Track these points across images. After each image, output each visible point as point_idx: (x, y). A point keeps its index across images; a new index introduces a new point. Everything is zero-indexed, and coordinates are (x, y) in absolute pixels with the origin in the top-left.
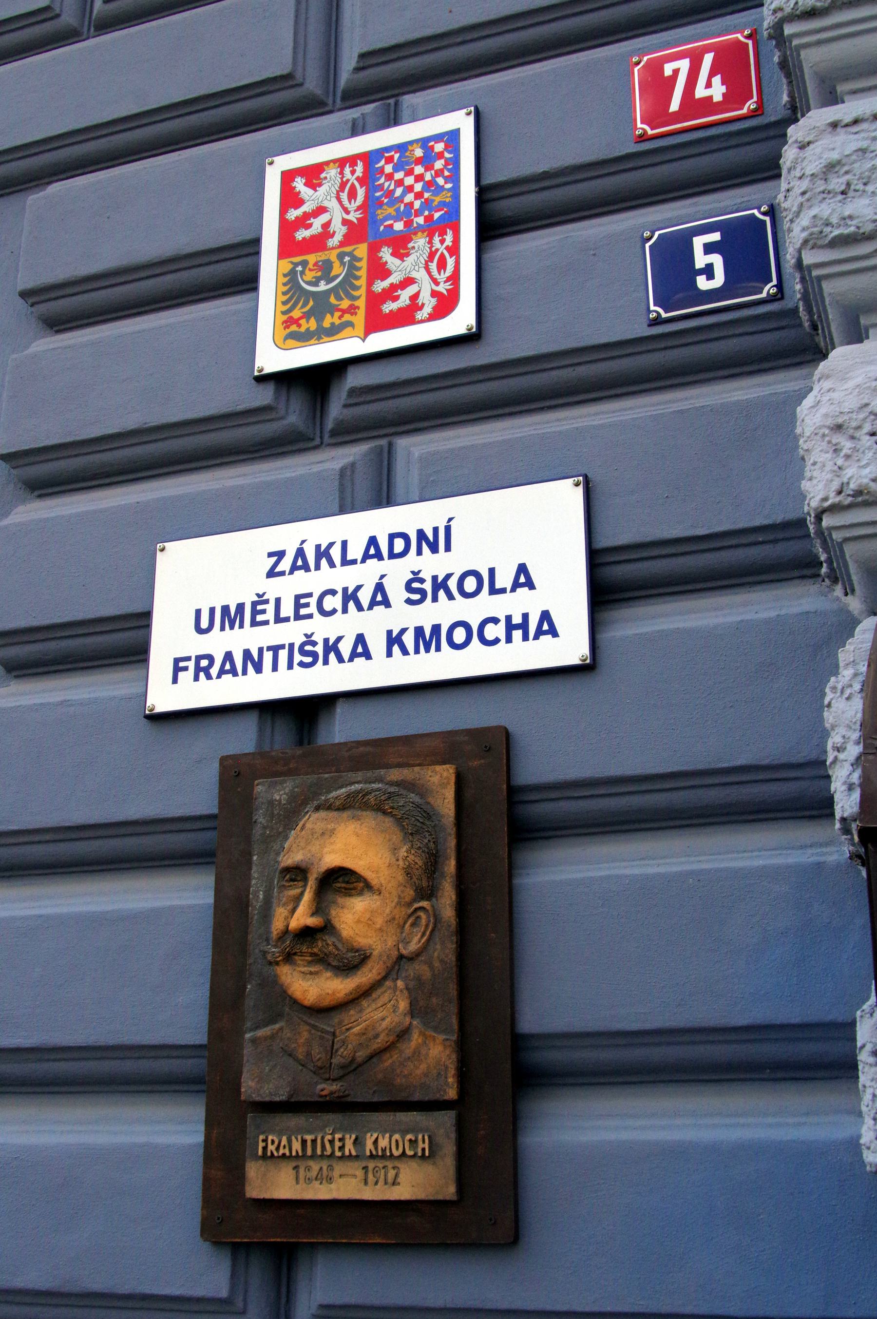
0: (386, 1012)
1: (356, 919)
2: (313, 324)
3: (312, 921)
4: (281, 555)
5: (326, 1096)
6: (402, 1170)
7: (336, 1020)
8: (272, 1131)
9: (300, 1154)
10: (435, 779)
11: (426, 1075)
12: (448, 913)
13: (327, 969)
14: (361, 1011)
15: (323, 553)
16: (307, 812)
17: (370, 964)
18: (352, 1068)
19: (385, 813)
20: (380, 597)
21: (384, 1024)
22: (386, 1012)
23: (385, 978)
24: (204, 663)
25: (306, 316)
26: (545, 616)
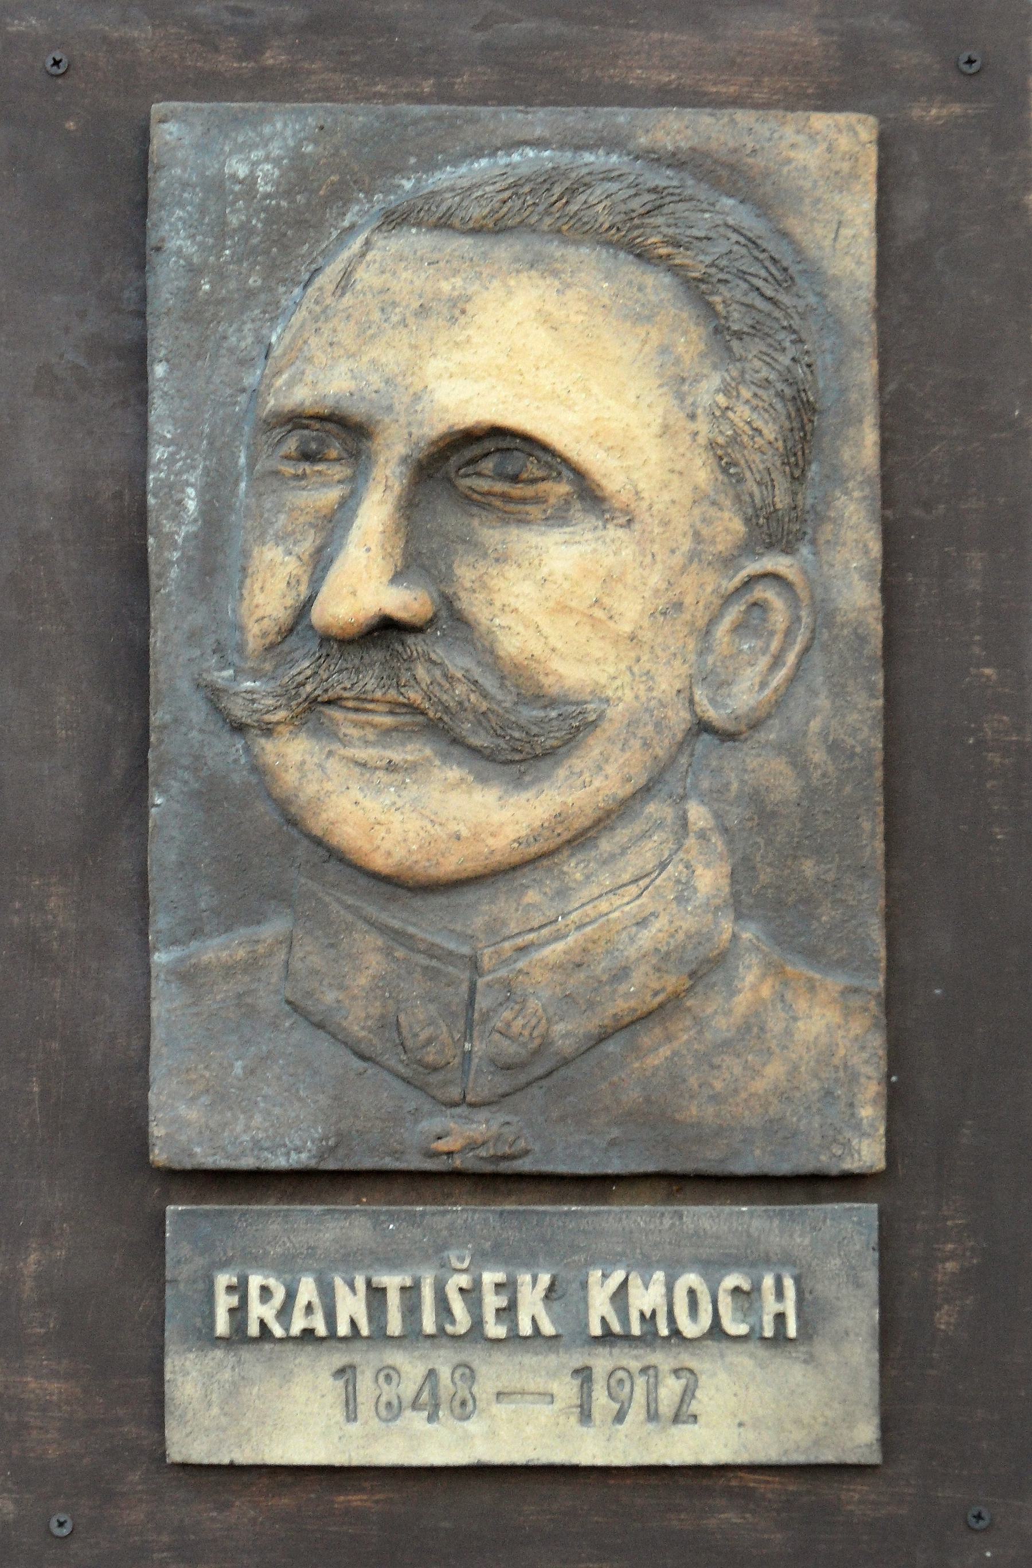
0: (651, 900)
1: (552, 601)
5: (450, 1154)
6: (703, 1379)
7: (479, 922)
8: (259, 1262)
9: (365, 1331)
10: (808, 157)
11: (784, 1096)
12: (858, 596)
13: (445, 757)
14: (562, 893)
16: (352, 229)
17: (595, 746)
18: (535, 1073)
19: (643, 256)
21: (646, 938)
22: (651, 900)
23: (645, 792)
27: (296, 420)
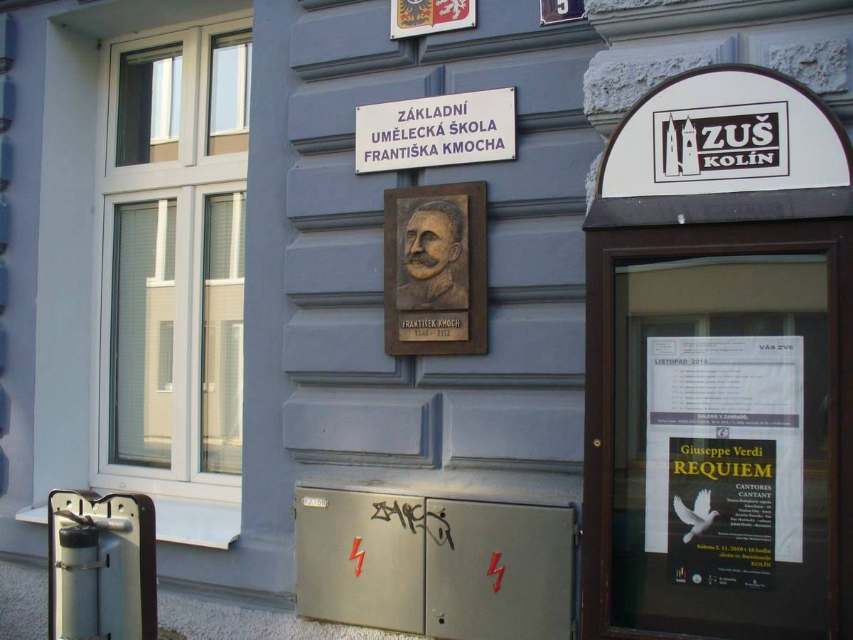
0: (444, 280)
2: (413, 19)
3: (419, 249)
4: (403, 113)
10: (461, 200)
11: (459, 300)
15: (419, 113)
18: (434, 299)
19: (443, 212)
20: (441, 131)
21: (445, 284)
22: (444, 280)
24: (377, 154)
25: (411, 14)
26: (500, 140)
27: (409, 232)
